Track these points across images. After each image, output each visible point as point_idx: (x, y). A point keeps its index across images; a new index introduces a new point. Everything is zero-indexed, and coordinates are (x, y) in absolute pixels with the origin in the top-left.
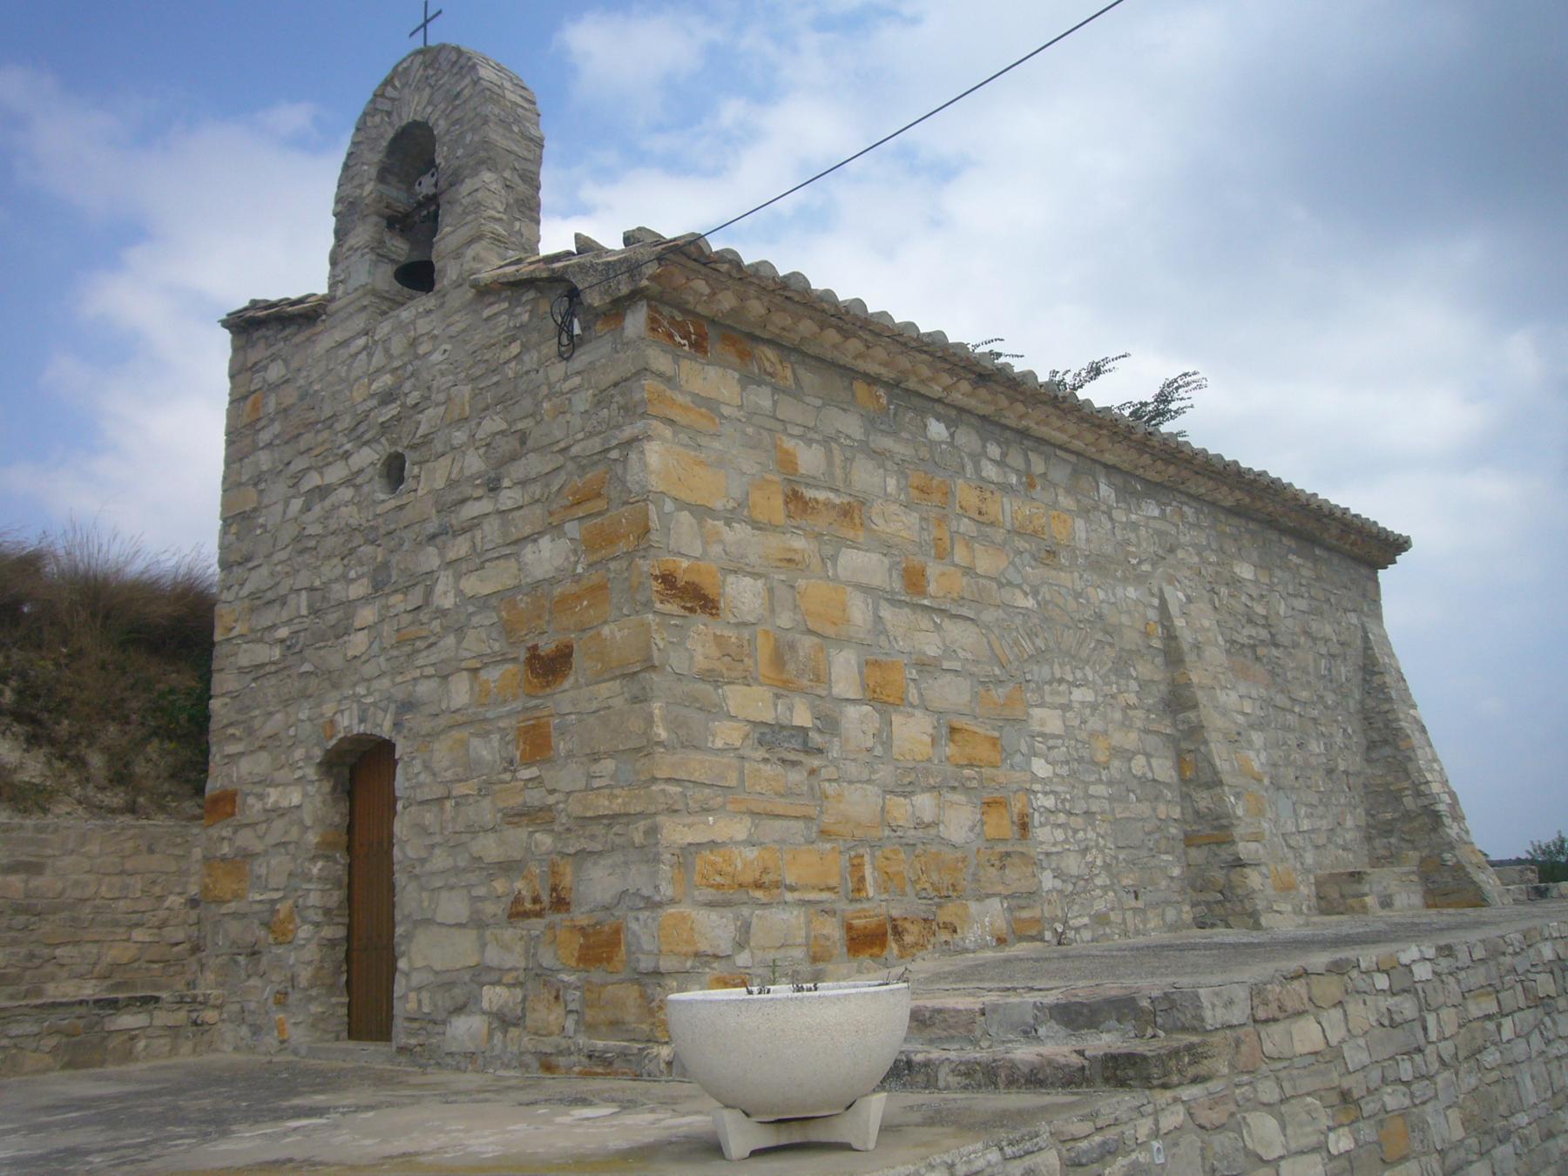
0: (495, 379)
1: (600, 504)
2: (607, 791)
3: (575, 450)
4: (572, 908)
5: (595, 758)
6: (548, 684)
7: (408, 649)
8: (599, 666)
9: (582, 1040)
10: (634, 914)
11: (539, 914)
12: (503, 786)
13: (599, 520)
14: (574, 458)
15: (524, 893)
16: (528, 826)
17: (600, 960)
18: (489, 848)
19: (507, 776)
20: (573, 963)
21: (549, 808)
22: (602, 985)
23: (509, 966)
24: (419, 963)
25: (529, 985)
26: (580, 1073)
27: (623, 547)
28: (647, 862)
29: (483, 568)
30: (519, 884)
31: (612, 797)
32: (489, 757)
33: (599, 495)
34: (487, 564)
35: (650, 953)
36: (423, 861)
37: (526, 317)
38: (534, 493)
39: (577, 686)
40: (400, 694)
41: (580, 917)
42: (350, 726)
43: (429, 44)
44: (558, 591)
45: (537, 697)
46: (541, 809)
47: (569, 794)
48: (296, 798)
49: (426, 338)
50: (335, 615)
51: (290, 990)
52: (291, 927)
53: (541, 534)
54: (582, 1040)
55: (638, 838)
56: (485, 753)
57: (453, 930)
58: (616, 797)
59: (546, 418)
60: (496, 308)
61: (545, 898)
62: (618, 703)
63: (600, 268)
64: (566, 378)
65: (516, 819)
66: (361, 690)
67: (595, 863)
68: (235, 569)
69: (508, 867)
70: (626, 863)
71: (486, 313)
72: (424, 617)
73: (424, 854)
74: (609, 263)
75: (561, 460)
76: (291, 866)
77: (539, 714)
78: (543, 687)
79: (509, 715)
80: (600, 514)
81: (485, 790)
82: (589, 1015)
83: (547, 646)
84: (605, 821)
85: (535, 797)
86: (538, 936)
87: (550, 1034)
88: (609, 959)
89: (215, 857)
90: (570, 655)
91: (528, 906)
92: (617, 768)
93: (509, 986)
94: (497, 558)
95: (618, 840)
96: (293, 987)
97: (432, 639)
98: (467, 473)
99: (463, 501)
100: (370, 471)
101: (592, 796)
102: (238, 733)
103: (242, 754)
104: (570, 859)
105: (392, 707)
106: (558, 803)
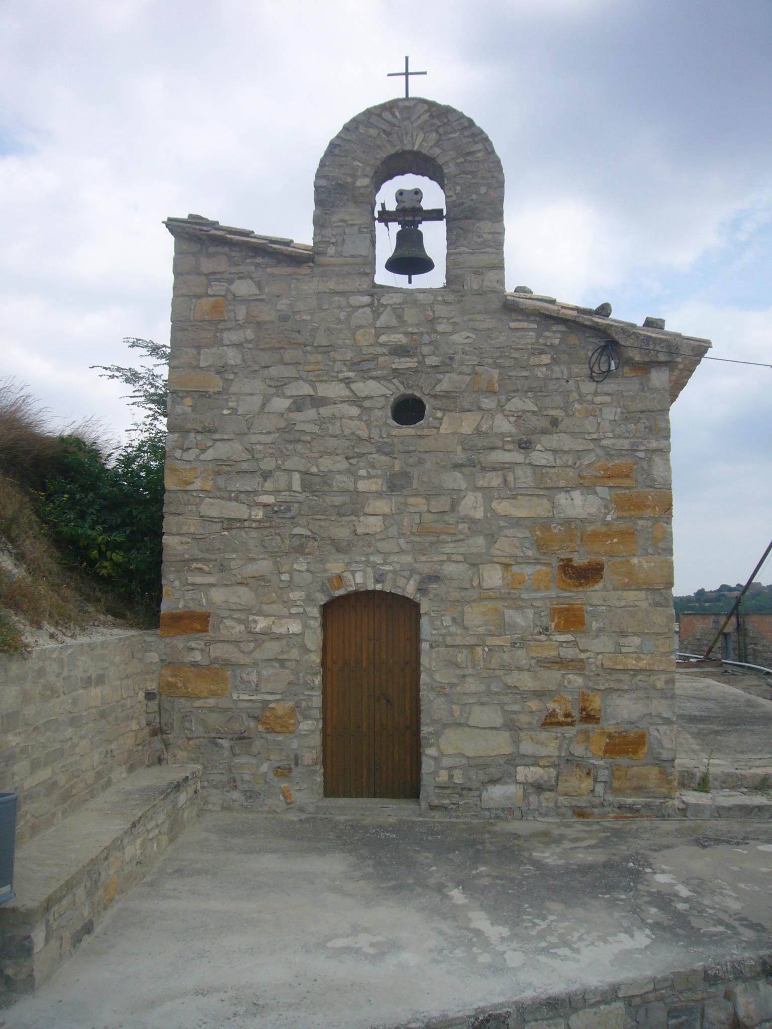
0: (525, 373)
1: (627, 482)
2: (635, 655)
3: (604, 442)
4: (601, 722)
5: (623, 634)
6: (581, 585)
7: (433, 539)
8: (627, 580)
9: (610, 798)
10: (655, 727)
11: (571, 724)
12: (539, 643)
13: (627, 491)
14: (602, 447)
15: (558, 710)
16: (559, 670)
17: (627, 753)
18: (527, 682)
19: (543, 638)
20: (601, 754)
21: (581, 660)
22: (628, 767)
23: (543, 755)
24: (451, 751)
25: (562, 766)
26: (615, 817)
27: (648, 513)
28: (666, 698)
29: (516, 498)
30: (551, 705)
31: (638, 659)
32: (523, 623)
33: (627, 476)
34: (519, 497)
35: (668, 749)
36: (453, 685)
37: (557, 341)
38: (568, 461)
39: (605, 589)
40: (426, 569)
41: (609, 726)
42: (364, 583)
43: (410, 96)
44: (590, 528)
45: (570, 591)
46: (572, 660)
47: (598, 654)
48: (295, 627)
49: (445, 321)
50: (341, 499)
51: (293, 766)
52: (292, 721)
53: (573, 488)
54: (610, 798)
55: (659, 685)
56: (519, 620)
57: (486, 731)
58: (643, 659)
59: (577, 414)
60: (524, 325)
61: (576, 714)
62: (644, 605)
63: (642, 337)
64: (596, 394)
65: (549, 665)
66: (378, 559)
67: (620, 696)
68: (192, 435)
69: (540, 694)
70: (648, 698)
71: (513, 325)
72: (450, 518)
73: (454, 681)
74: (650, 337)
75: (592, 446)
76: (292, 678)
77: (573, 602)
78: (576, 586)
79: (542, 598)
80: (627, 488)
81: (519, 643)
82: (616, 784)
83: (580, 560)
84: (632, 673)
85: (568, 653)
86: (571, 738)
87: (581, 795)
88: (635, 752)
89: (183, 663)
90: (602, 569)
91: (561, 719)
92: (642, 642)
93: (543, 767)
94: (530, 495)
95: (640, 684)
96: (297, 764)
97: (461, 537)
98: (495, 430)
99: (493, 448)
100: (381, 402)
101: (620, 657)
102: (206, 568)
103: (214, 585)
104: (600, 693)
105: (417, 577)
106: (589, 658)
